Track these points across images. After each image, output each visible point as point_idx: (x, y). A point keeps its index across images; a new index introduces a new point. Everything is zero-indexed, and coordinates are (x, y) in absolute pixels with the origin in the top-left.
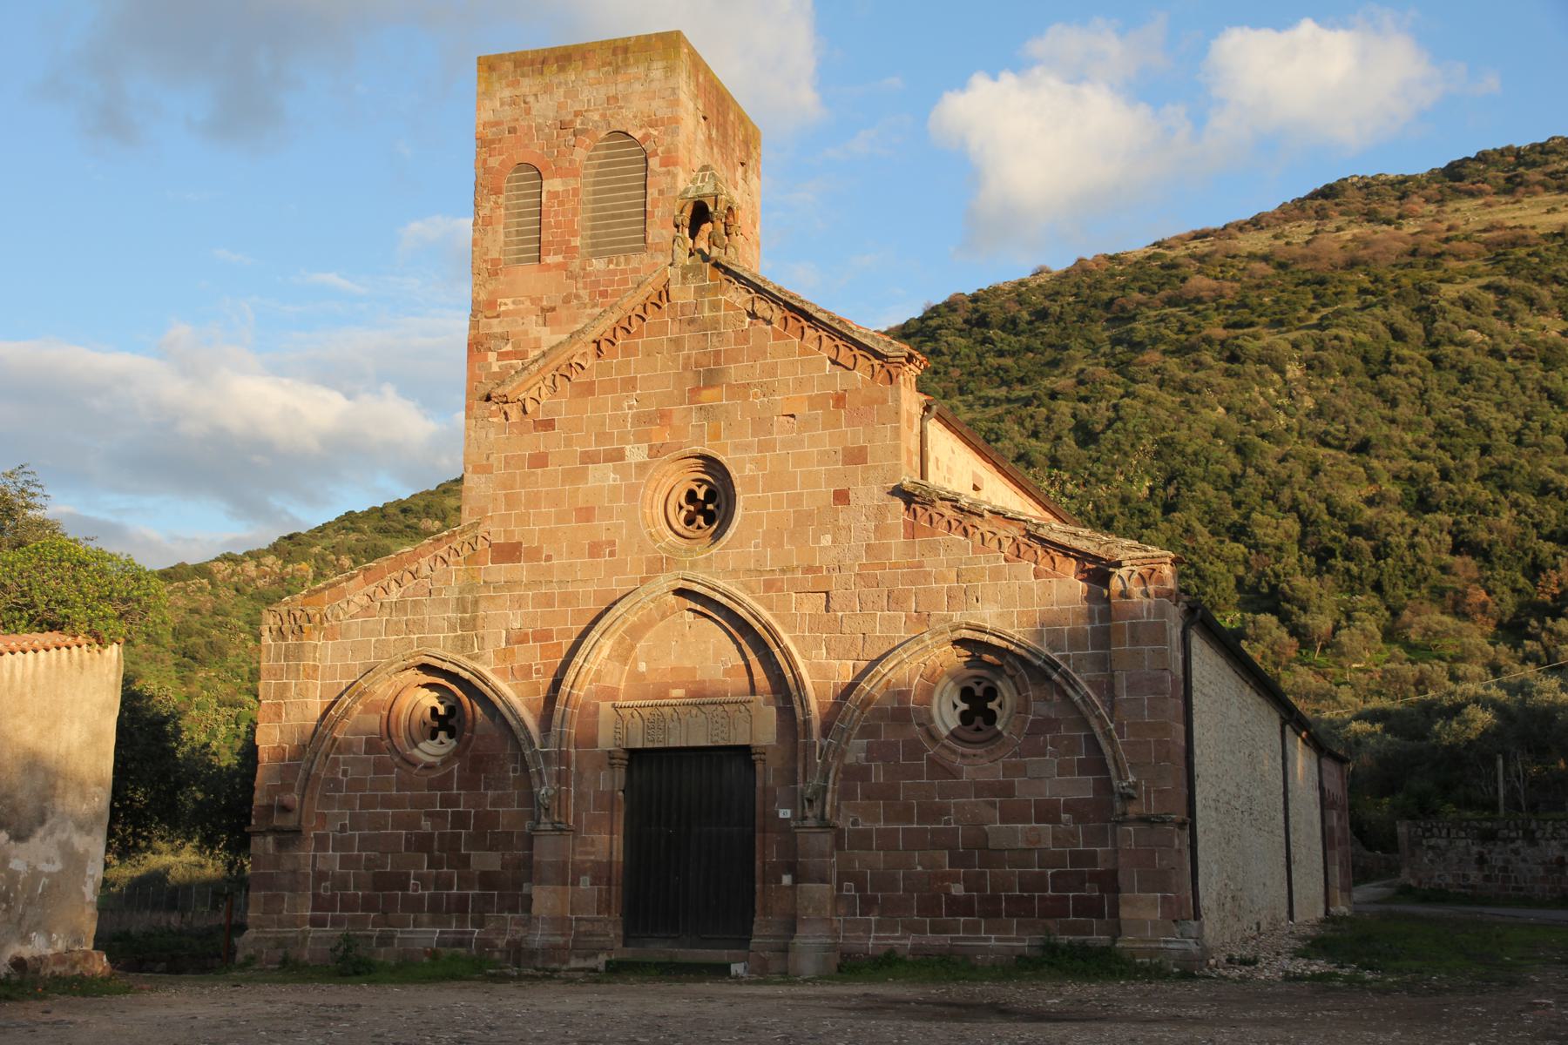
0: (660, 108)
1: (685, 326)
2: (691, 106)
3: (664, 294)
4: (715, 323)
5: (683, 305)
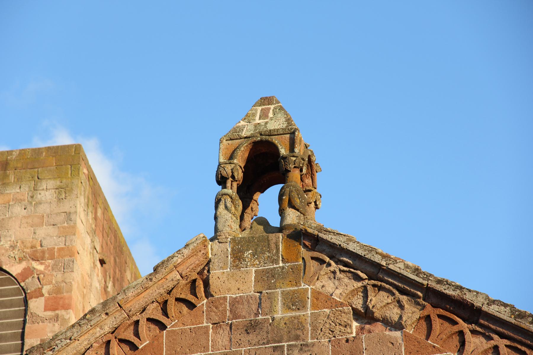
0: (48, 237)
1: (237, 336)
2: (88, 240)
3: (200, 283)
4: (295, 329)
5: (235, 302)
